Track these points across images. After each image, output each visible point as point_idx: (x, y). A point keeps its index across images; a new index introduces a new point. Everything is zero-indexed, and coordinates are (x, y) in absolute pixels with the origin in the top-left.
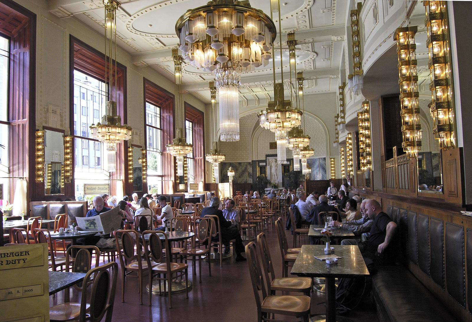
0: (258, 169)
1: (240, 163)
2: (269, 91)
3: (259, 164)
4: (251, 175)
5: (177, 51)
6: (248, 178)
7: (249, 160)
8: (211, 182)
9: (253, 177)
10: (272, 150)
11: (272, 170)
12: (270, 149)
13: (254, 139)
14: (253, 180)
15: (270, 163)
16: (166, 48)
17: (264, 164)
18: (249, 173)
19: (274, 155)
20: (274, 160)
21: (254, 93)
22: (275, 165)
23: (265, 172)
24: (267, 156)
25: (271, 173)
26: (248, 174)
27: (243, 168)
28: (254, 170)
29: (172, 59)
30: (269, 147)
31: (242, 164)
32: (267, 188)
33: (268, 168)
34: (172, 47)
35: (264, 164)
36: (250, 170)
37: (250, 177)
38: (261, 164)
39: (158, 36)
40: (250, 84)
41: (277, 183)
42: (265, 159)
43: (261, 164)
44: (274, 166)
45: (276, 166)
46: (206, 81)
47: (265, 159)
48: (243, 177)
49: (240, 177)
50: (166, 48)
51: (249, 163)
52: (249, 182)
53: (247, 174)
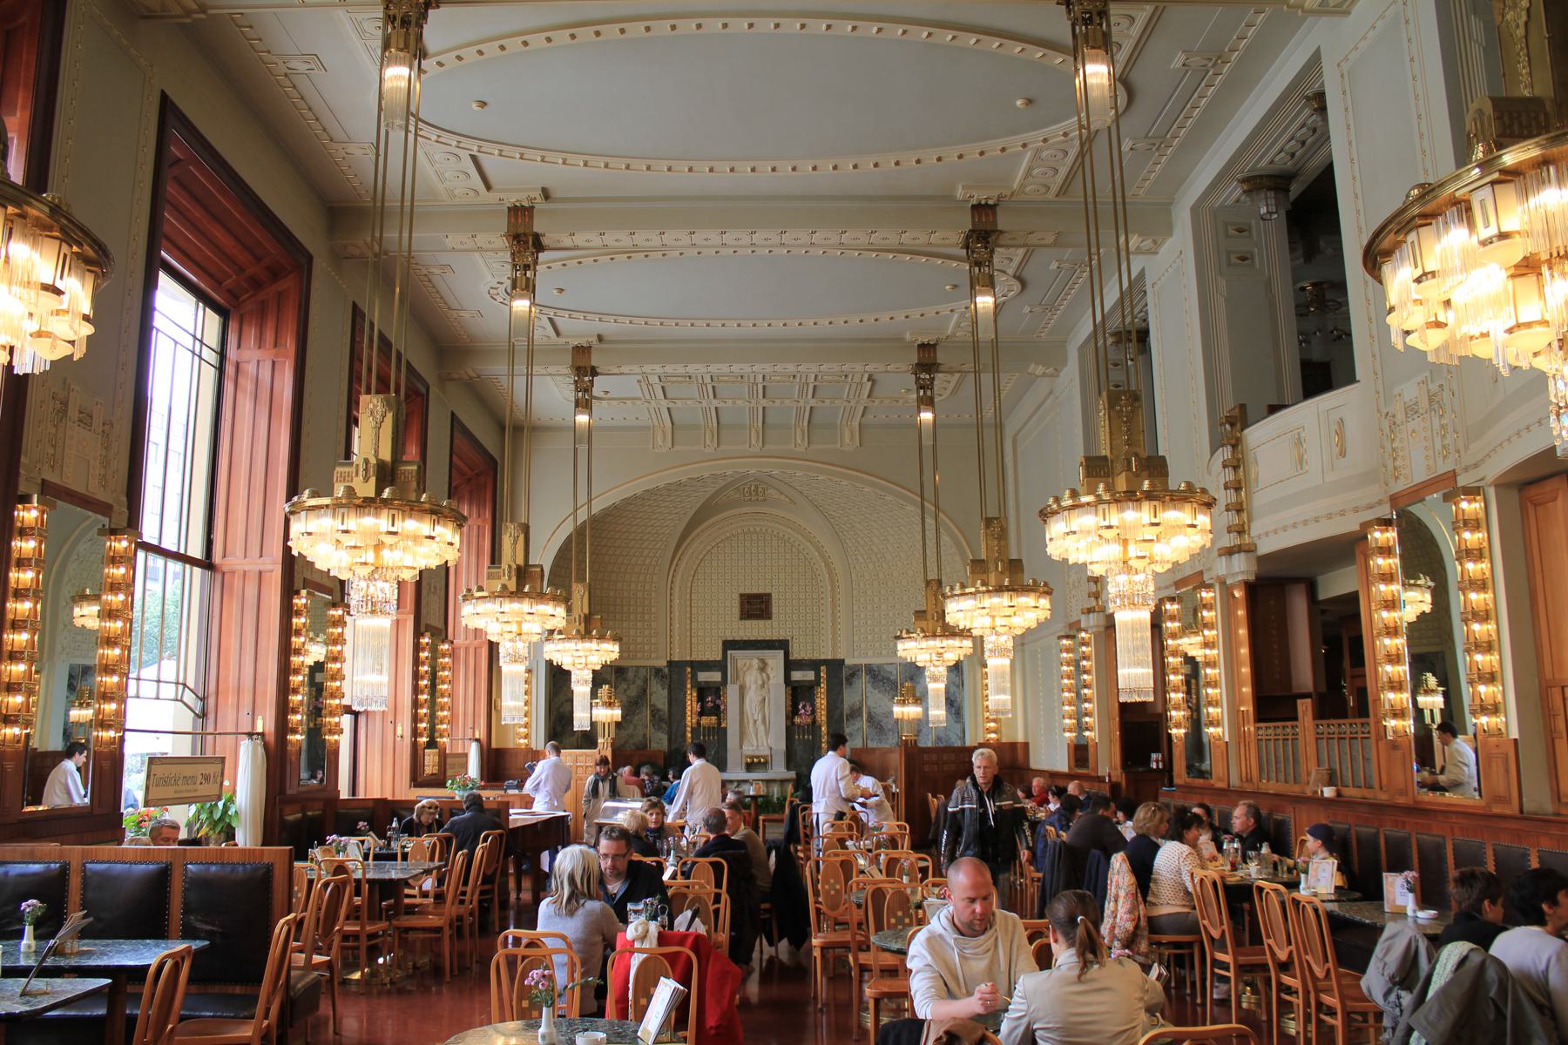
2: (673, 400)
3: (694, 676)
4: (661, 720)
5: (531, 217)
6: (650, 731)
8: (511, 746)
9: (670, 727)
10: (748, 622)
11: (747, 701)
13: (679, 577)
14: (670, 740)
16: (491, 197)
17: (716, 676)
18: (655, 712)
20: (755, 662)
21: (715, 403)
23: (717, 711)
24: (729, 645)
25: (742, 713)
26: (653, 716)
28: (676, 702)
29: (502, 242)
30: (736, 611)
31: (630, 675)
33: (732, 692)
34: (512, 199)
35: (716, 676)
36: (659, 696)
37: (660, 728)
38: (703, 677)
39: (486, 147)
40: (669, 369)
41: (767, 752)
42: (719, 658)
43: (703, 677)
45: (763, 686)
46: (562, 340)
47: (719, 658)
50: (491, 197)
51: (658, 671)
52: (654, 746)
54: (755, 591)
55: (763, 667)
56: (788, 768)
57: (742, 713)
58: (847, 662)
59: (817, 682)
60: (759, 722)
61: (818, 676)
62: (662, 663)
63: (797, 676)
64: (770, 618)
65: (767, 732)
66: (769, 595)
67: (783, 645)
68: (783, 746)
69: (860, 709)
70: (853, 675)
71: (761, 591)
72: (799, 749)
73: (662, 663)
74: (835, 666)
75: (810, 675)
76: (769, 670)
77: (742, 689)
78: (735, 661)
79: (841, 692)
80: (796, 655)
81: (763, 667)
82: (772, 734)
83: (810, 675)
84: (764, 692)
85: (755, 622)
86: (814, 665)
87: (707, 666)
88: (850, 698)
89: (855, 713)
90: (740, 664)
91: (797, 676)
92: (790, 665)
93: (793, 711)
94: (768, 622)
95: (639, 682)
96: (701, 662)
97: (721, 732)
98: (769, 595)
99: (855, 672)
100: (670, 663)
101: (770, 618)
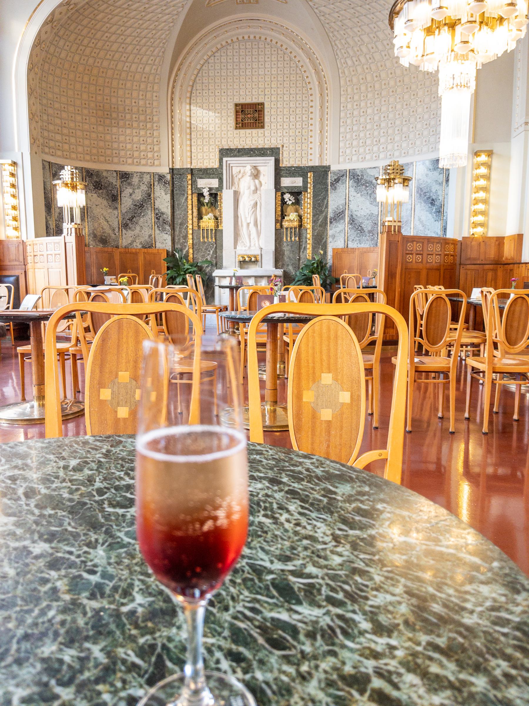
0: (191, 200)
1: (125, 176)
3: (194, 183)
4: (165, 222)
7: (160, 165)
9: (173, 229)
10: (242, 131)
12: (236, 128)
15: (236, 180)
17: (214, 183)
18: (159, 216)
19: (251, 150)
20: (248, 169)
22: (253, 188)
24: (225, 152)
25: (236, 217)
27: (138, 196)
31: (135, 180)
32: (221, 268)
33: (226, 198)
35: (214, 183)
36: (163, 200)
37: (164, 230)
44: (247, 192)
47: (216, 165)
48: (138, 228)
49: (126, 226)
51: (161, 177)
53: (150, 216)
54: (248, 100)
55: (256, 175)
56: (276, 267)
57: (236, 217)
58: (332, 168)
59: (305, 188)
60: (252, 225)
61: (305, 182)
62: (164, 170)
63: (286, 182)
64: (263, 127)
65: (259, 234)
66: (262, 104)
67: (274, 152)
68: (272, 247)
69: (343, 212)
70: (337, 180)
71: (255, 101)
72: (286, 249)
73: (164, 170)
74: (321, 173)
75: (298, 182)
76: (262, 178)
77: (236, 195)
78: (229, 167)
79: (326, 197)
80: (285, 163)
81: (256, 175)
82: (262, 236)
83: (298, 182)
84: (256, 197)
85: (248, 131)
86: (300, 171)
87: (206, 173)
88: (334, 201)
89: (339, 216)
90: (235, 170)
91: (286, 182)
92: (279, 172)
93: (282, 216)
94: (260, 131)
95: (144, 188)
96: (200, 170)
97: (217, 233)
98: (262, 104)
99: (340, 177)
100: (172, 170)
101: (263, 127)
